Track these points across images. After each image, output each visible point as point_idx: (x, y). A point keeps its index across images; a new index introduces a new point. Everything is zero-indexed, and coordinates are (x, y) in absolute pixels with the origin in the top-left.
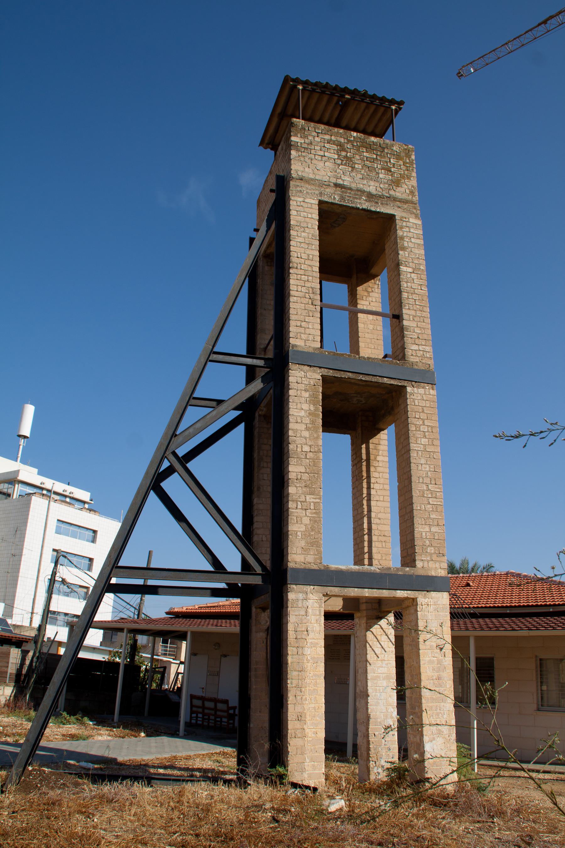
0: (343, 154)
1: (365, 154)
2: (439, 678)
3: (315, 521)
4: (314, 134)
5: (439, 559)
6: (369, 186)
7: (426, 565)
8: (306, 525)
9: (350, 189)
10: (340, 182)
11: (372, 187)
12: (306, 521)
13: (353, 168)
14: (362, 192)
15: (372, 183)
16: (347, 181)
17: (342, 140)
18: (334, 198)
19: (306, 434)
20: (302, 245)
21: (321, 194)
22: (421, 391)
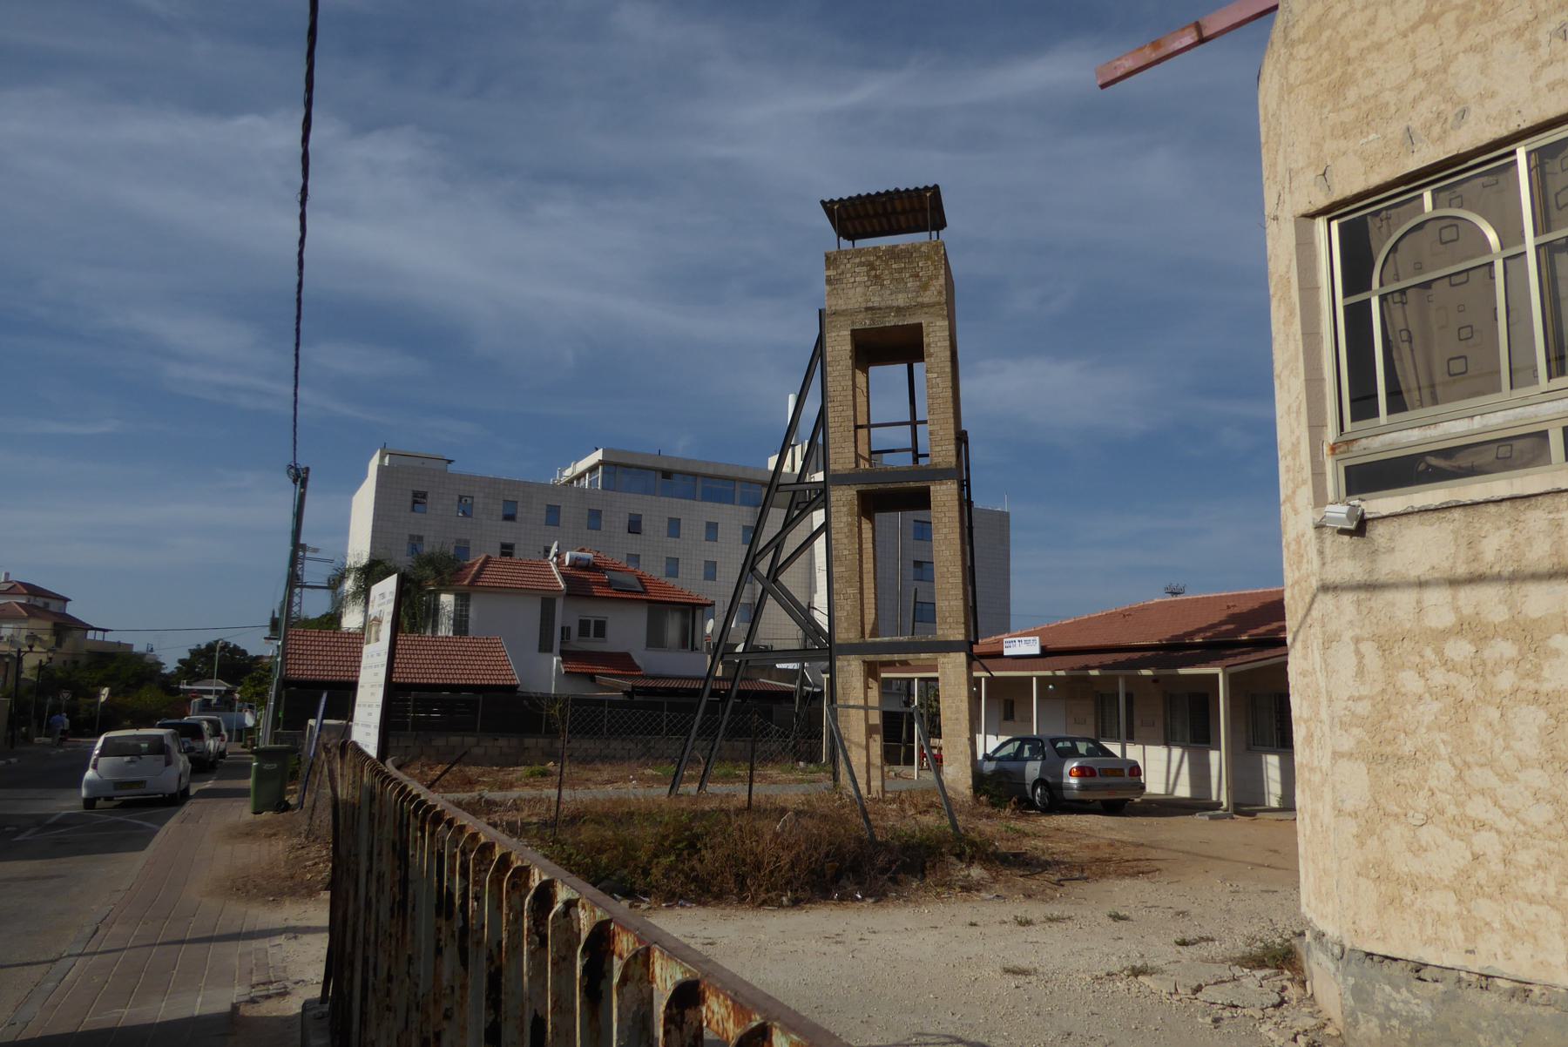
11: (901, 300)
14: (890, 308)
16: (876, 301)
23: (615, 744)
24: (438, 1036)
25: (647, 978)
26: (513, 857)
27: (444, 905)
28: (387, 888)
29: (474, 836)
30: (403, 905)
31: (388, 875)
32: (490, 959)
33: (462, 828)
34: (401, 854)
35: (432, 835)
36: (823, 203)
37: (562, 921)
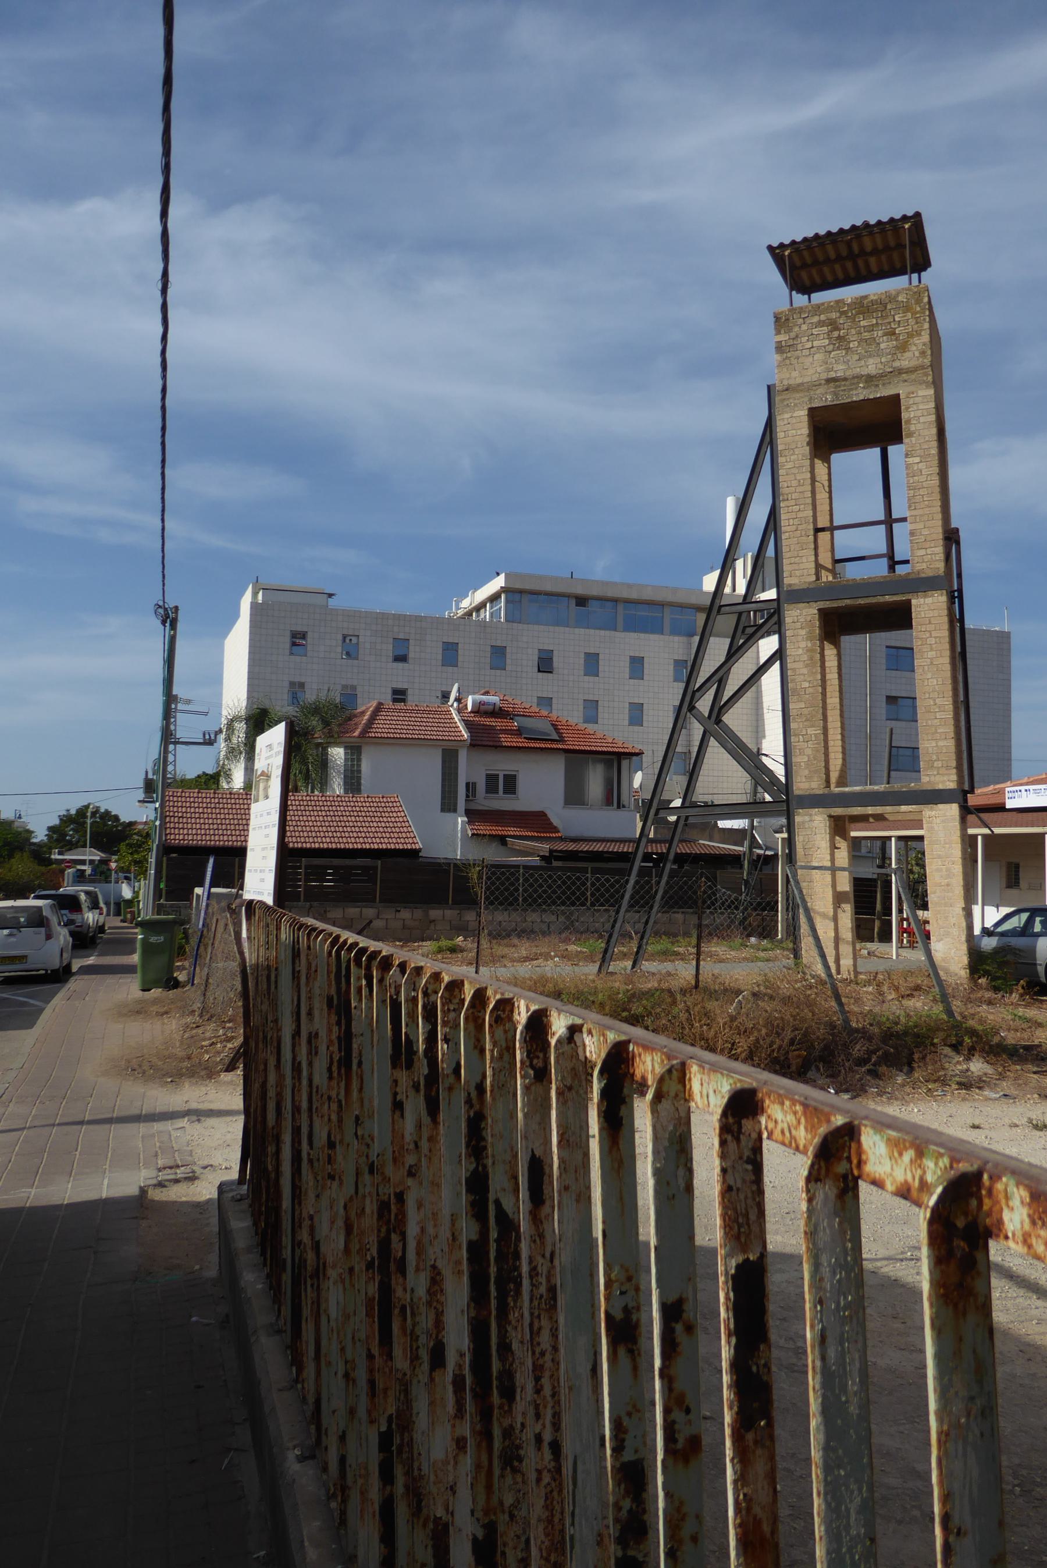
0: (836, 334)
1: (862, 323)
2: (948, 885)
4: (801, 320)
7: (932, 779)
8: (808, 756)
9: (845, 379)
10: (833, 375)
11: (872, 366)
12: (809, 752)
13: (848, 349)
14: (859, 377)
15: (871, 361)
16: (840, 370)
17: (834, 315)
19: (805, 671)
21: (811, 399)
22: (929, 600)
23: (533, 917)
24: (400, 1197)
25: (684, 1096)
26: (489, 992)
27: (402, 1053)
28: (323, 1049)
29: (436, 977)
30: (346, 1062)
31: (323, 1034)
32: (469, 1101)
33: (418, 970)
34: (341, 1008)
35: (381, 981)
36: (770, 248)
37: (567, 1048)
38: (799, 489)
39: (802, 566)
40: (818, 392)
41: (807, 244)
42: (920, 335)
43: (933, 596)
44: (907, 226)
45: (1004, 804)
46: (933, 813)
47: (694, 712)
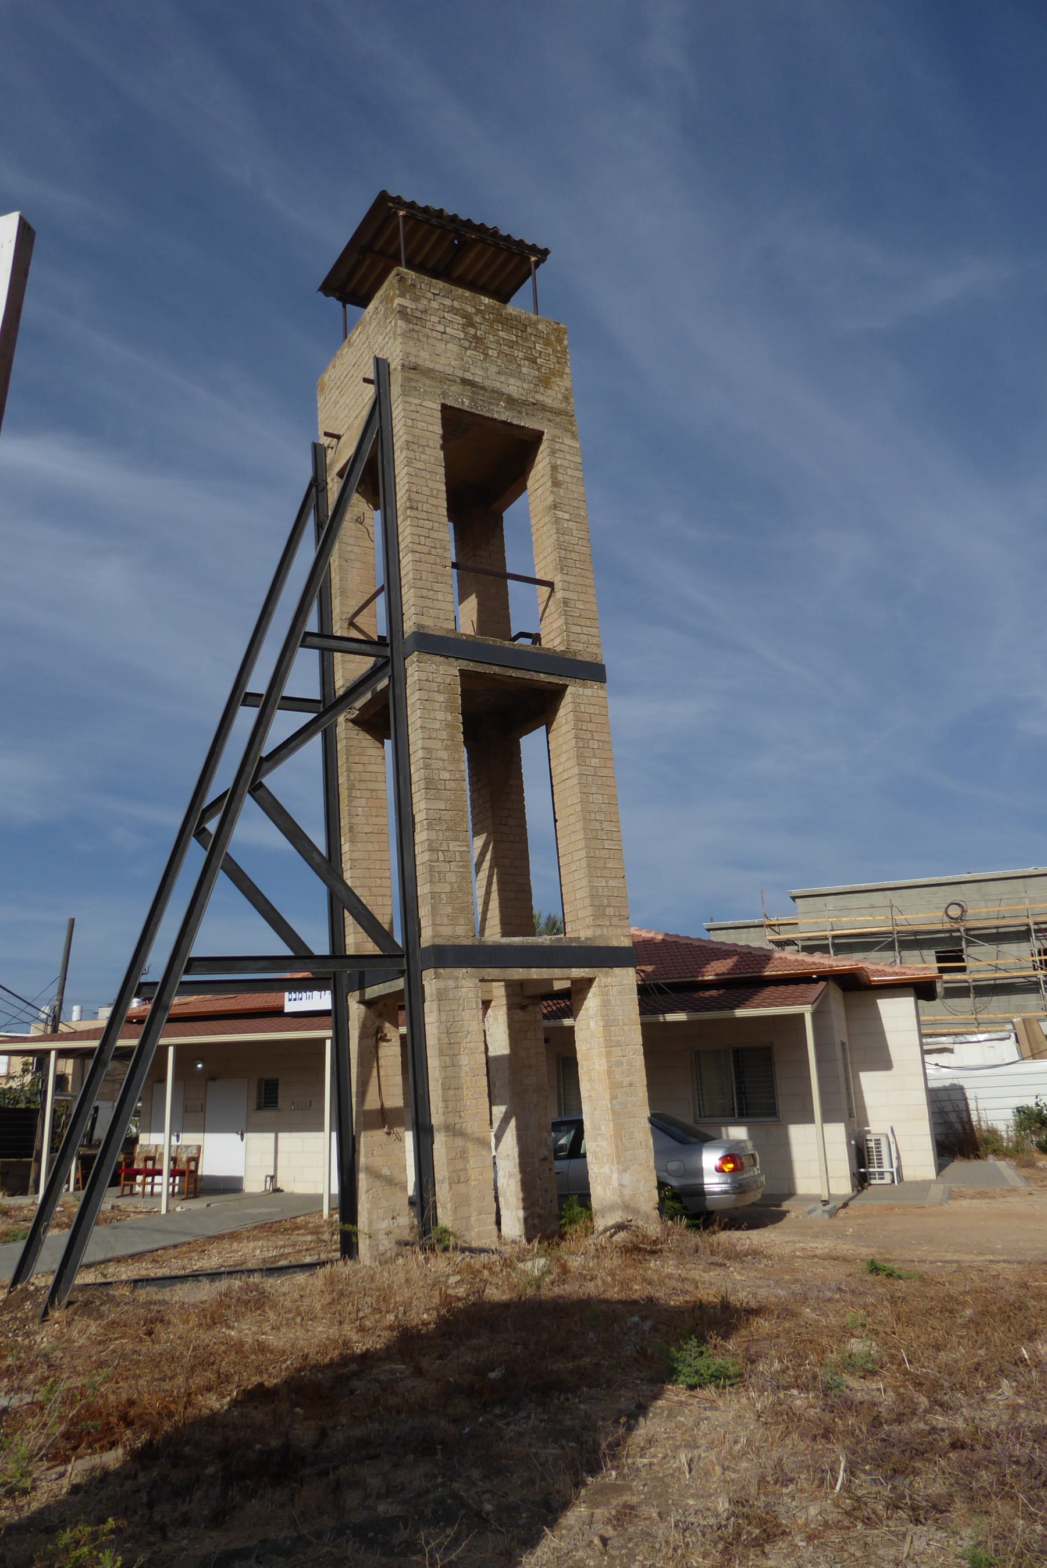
0: (472, 331)
2: (631, 1085)
3: (464, 878)
4: (430, 295)
5: (621, 923)
6: (509, 385)
8: (451, 883)
9: (484, 388)
10: (468, 376)
11: (514, 388)
12: (451, 877)
15: (512, 381)
16: (477, 374)
17: (470, 309)
18: (463, 403)
19: (444, 755)
20: (424, 473)
21: (444, 394)
22: (588, 692)
38: (432, 501)
39: (437, 605)
40: (452, 389)
41: (425, 216)
42: (562, 376)
43: (591, 687)
44: (533, 259)
45: (283, 1007)
46: (609, 980)
47: (260, 793)
